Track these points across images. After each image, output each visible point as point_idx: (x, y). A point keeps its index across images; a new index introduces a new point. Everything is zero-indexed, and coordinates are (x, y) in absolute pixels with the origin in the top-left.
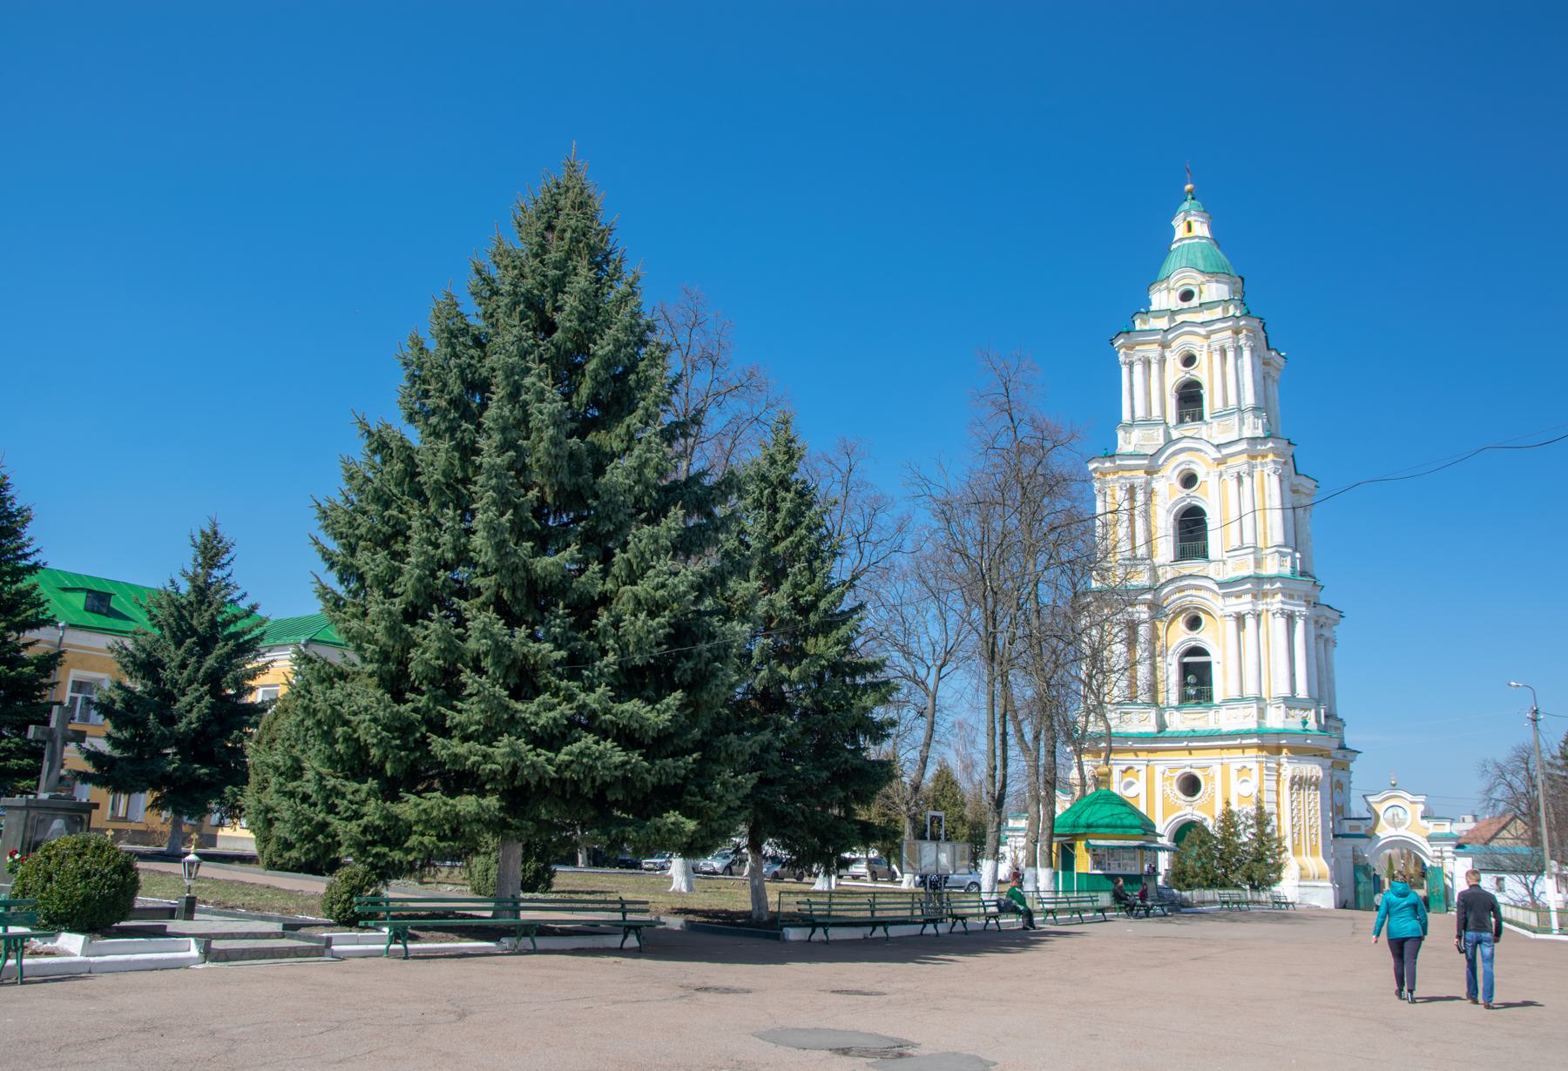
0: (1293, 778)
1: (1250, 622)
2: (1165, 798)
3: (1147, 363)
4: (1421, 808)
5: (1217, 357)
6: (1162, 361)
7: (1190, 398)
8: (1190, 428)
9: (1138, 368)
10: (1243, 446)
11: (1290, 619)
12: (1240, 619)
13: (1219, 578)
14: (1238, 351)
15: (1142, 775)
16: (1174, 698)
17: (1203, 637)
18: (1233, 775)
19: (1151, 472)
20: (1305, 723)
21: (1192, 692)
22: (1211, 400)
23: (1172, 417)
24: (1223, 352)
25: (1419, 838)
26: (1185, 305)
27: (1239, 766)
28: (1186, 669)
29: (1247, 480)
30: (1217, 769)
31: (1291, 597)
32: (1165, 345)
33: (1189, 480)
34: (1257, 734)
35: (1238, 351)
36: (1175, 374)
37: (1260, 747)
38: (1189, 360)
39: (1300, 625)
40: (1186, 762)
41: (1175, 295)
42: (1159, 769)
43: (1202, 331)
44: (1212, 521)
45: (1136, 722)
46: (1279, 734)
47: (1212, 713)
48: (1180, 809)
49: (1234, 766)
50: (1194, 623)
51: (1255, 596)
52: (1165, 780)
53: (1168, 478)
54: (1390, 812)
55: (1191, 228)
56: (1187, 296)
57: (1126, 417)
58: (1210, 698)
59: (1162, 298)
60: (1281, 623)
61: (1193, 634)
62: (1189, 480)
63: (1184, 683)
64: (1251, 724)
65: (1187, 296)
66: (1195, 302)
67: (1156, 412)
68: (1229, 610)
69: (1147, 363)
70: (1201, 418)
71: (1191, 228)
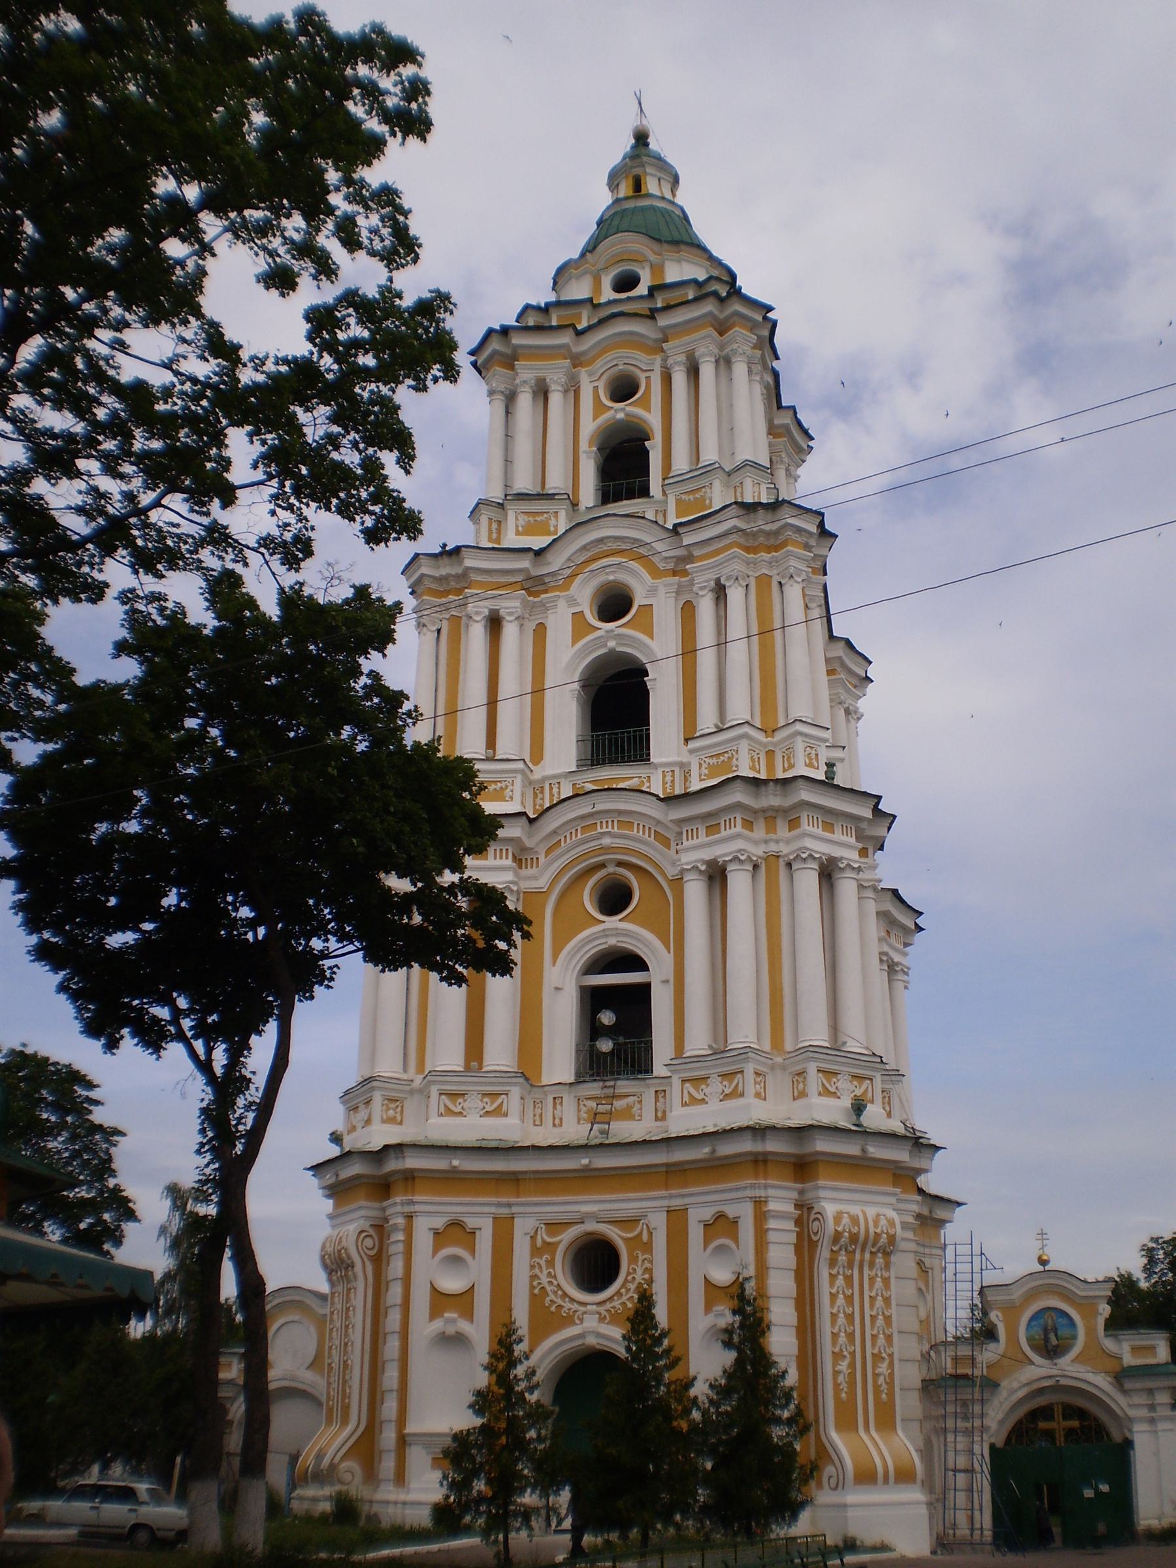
0: (837, 1237)
1: (739, 883)
2: (537, 1299)
3: (542, 392)
4: (1105, 1310)
5: (680, 380)
6: (573, 390)
9: (525, 402)
11: (828, 873)
14: (724, 362)
15: (485, 1242)
16: (566, 1073)
18: (695, 1234)
19: (534, 585)
20: (858, 1108)
21: (605, 1045)
23: (588, 494)
25: (1100, 1382)
26: (624, 296)
27: (708, 1213)
28: (594, 1000)
30: (659, 1221)
31: (828, 827)
32: (577, 361)
33: (615, 604)
34: (759, 1131)
35: (724, 362)
37: (760, 1162)
38: (624, 389)
40: (593, 1211)
41: (607, 282)
42: (523, 1228)
46: (802, 1132)
48: (569, 1321)
49: (699, 1215)
50: (614, 899)
51: (748, 824)
52: (536, 1251)
53: (572, 602)
54: (1042, 1321)
58: (649, 1070)
60: (808, 881)
61: (613, 922)
62: (615, 604)
63: (592, 1030)
65: (626, 283)
66: (642, 289)
68: (687, 859)
69: (542, 392)
70: (644, 492)
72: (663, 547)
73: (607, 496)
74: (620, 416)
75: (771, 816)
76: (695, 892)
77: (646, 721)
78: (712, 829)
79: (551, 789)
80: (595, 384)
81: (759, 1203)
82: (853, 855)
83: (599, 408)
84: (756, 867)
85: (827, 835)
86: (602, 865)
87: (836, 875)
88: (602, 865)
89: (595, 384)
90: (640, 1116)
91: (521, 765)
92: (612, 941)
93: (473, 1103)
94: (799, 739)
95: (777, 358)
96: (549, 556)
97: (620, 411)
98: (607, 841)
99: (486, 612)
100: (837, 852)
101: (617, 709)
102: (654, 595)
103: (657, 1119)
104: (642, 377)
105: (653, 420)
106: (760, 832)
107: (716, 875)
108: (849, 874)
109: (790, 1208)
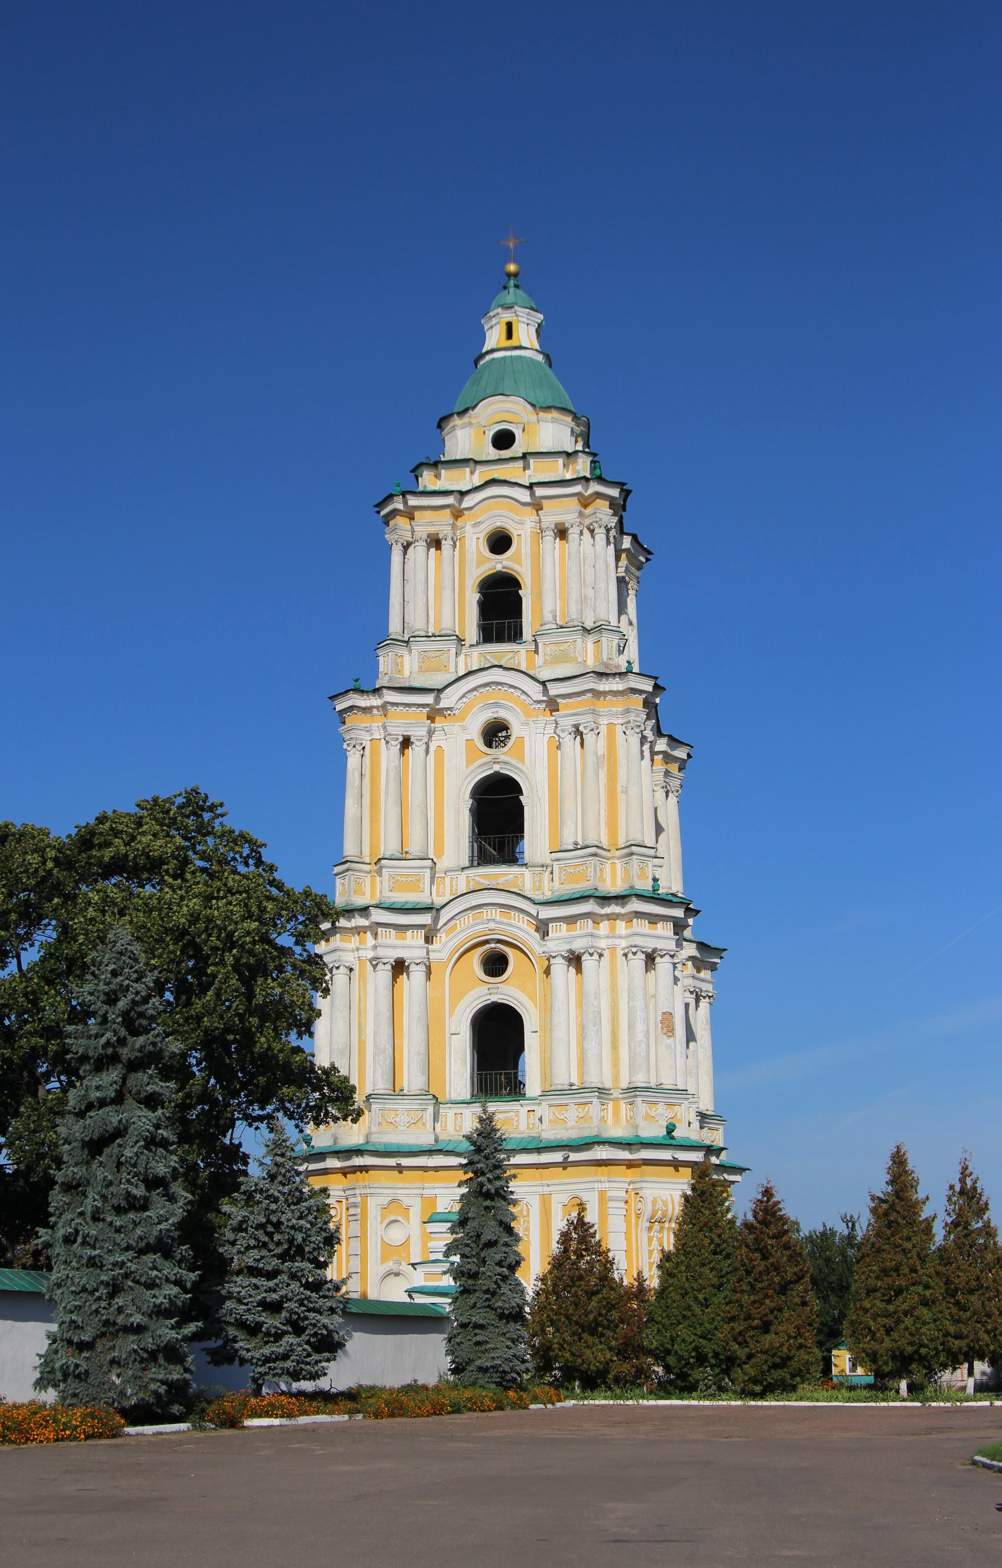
3: (436, 543)
7: (500, 608)
8: (501, 651)
11: (650, 959)
13: (538, 897)
17: (509, 991)
38: (500, 542)
47: (523, 1111)
50: (496, 965)
55: (513, 330)
56: (504, 440)
57: (394, 627)
59: (466, 438)
62: (495, 733)
65: (504, 440)
71: (513, 330)
74: (499, 567)
75: (612, 917)
77: (523, 832)
79: (451, 881)
80: (478, 536)
81: (602, 1193)
83: (481, 561)
84: (601, 955)
86: (487, 942)
87: (658, 960)
88: (487, 942)
89: (478, 536)
90: (518, 1126)
91: (429, 863)
95: (624, 510)
97: (500, 563)
99: (401, 739)
100: (660, 944)
101: (498, 817)
103: (528, 1128)
108: (667, 958)
109: (623, 1194)
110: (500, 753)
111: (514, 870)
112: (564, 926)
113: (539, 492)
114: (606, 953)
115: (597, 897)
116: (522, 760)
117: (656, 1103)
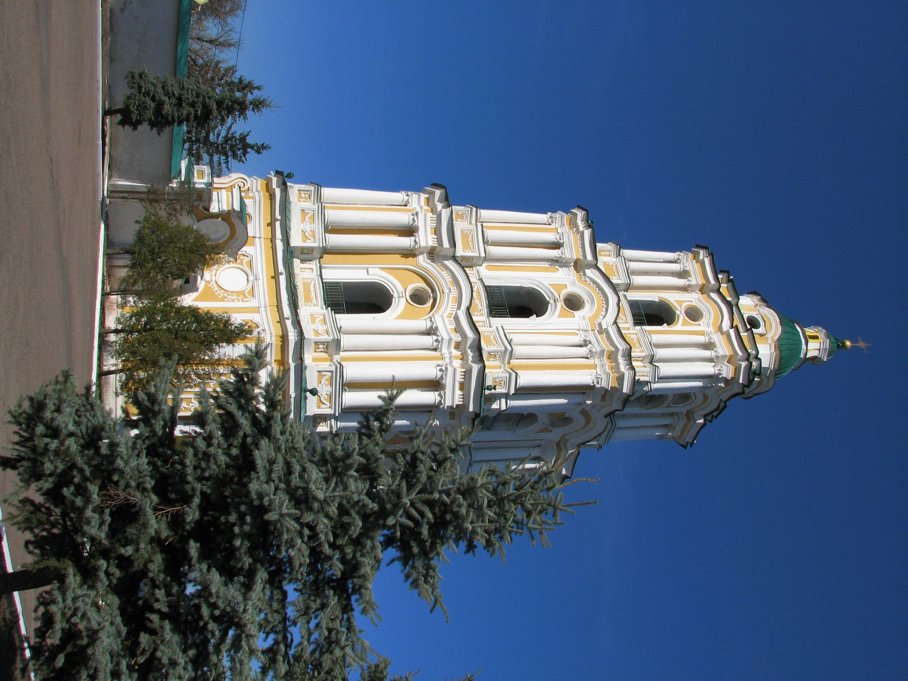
1: (429, 340)
3: (683, 274)
5: (701, 339)
10: (621, 346)
12: (431, 332)
20: (314, 392)
22: (658, 333)
24: (709, 346)
29: (583, 351)
30: (253, 303)
33: (573, 303)
36: (678, 301)
39: (428, 397)
41: (754, 314)
43: (726, 324)
44: (532, 321)
45: (302, 226)
50: (418, 298)
62: (573, 303)
64: (308, 334)
65: (753, 323)
67: (637, 280)
72: (607, 322)
73: (634, 305)
74: (678, 312)
75: (463, 358)
76: (422, 324)
78: (456, 330)
82: (448, 403)
83: (680, 303)
85: (457, 385)
91: (483, 255)
92: (395, 295)
93: (308, 227)
94: (508, 375)
96: (596, 272)
97: (680, 312)
98: (446, 291)
100: (448, 391)
102: (580, 319)
104: (701, 322)
105: (678, 326)
106: (456, 353)
107: (431, 332)
110: (560, 304)
111: (485, 310)
112: (453, 327)
113: (732, 332)
114: (437, 354)
115: (479, 341)
116: (560, 316)
117: (331, 385)
